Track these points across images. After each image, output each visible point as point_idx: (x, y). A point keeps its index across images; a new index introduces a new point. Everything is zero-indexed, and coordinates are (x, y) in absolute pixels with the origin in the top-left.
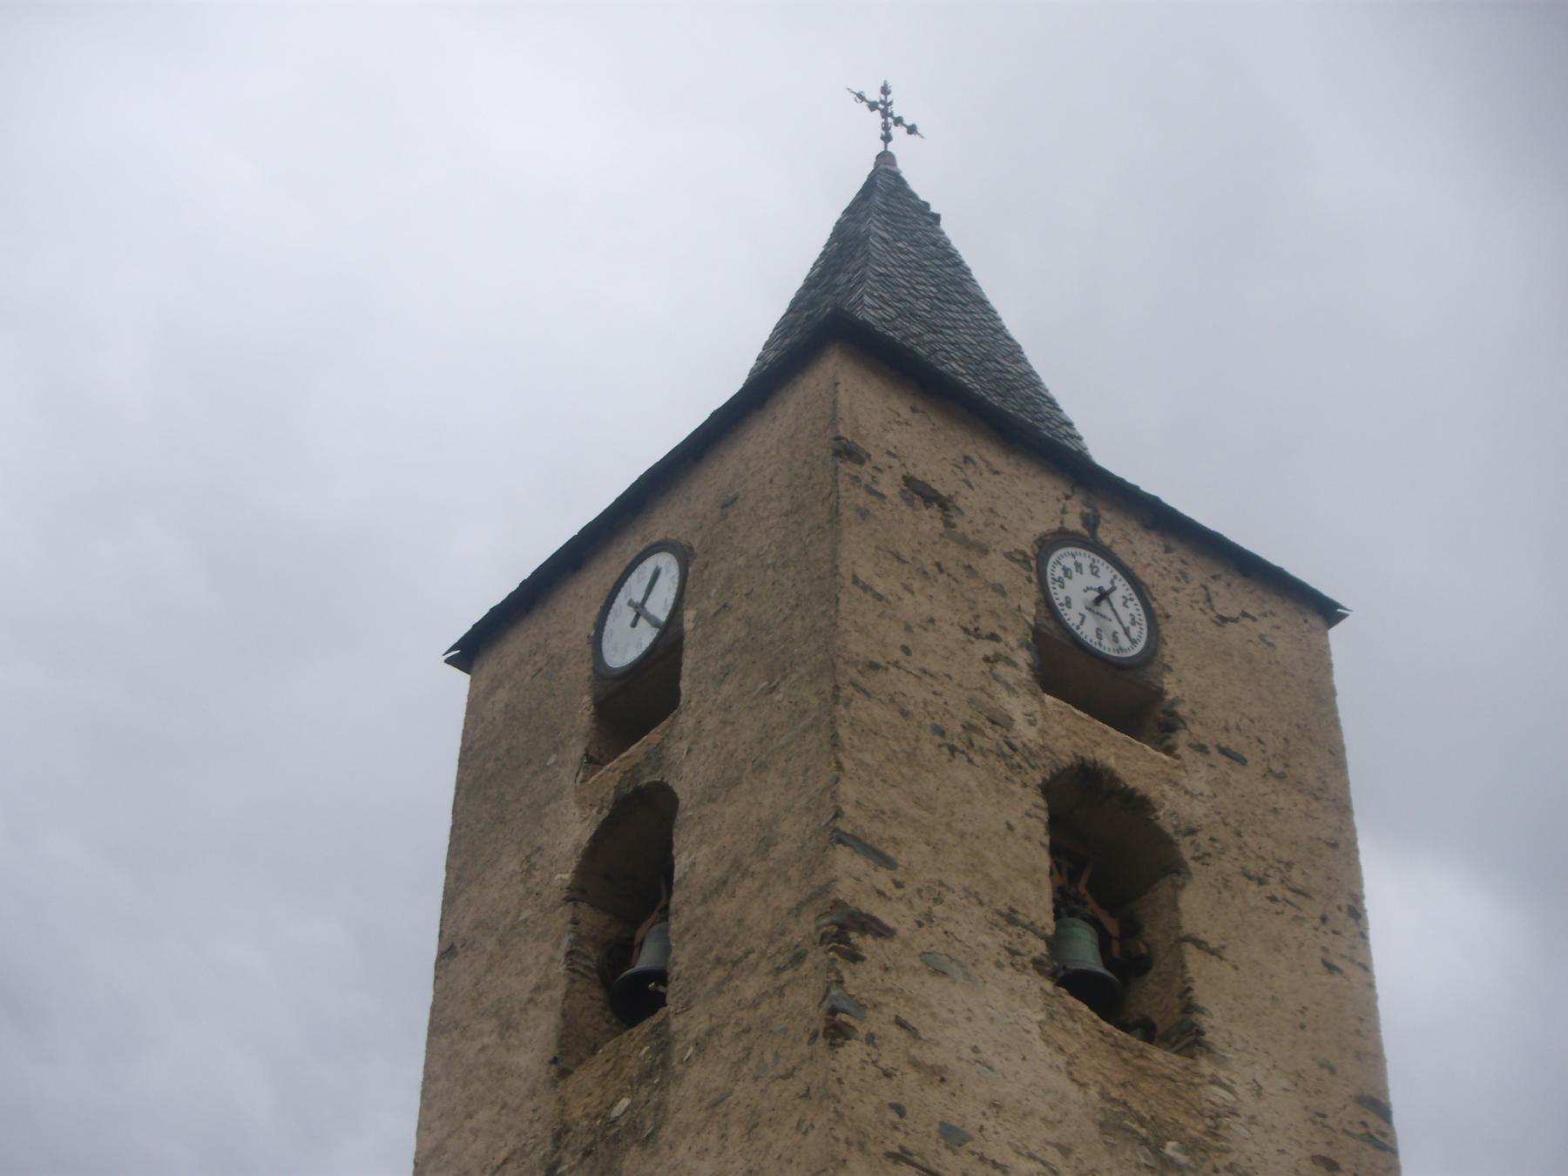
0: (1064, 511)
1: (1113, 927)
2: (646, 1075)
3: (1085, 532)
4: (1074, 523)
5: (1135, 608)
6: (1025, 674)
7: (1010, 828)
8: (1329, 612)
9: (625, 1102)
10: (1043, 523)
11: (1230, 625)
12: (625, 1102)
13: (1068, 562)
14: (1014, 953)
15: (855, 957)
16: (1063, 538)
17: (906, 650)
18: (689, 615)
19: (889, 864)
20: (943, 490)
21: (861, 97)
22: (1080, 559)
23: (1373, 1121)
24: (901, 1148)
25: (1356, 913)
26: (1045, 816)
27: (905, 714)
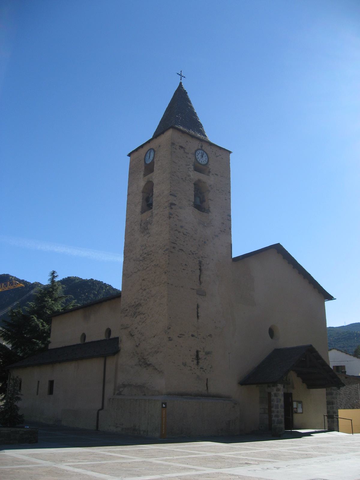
0: (198, 146)
2: (151, 216)
3: (201, 148)
4: (200, 147)
5: (206, 157)
6: (192, 169)
7: (190, 189)
8: (230, 152)
9: (148, 219)
11: (218, 157)
12: (148, 219)
14: (189, 205)
15: (172, 208)
16: (198, 149)
17: (179, 169)
18: (155, 160)
19: (176, 196)
20: (184, 146)
21: (178, 74)
22: (200, 152)
24: (176, 230)
25: (230, 192)
26: (194, 187)
27: (178, 177)
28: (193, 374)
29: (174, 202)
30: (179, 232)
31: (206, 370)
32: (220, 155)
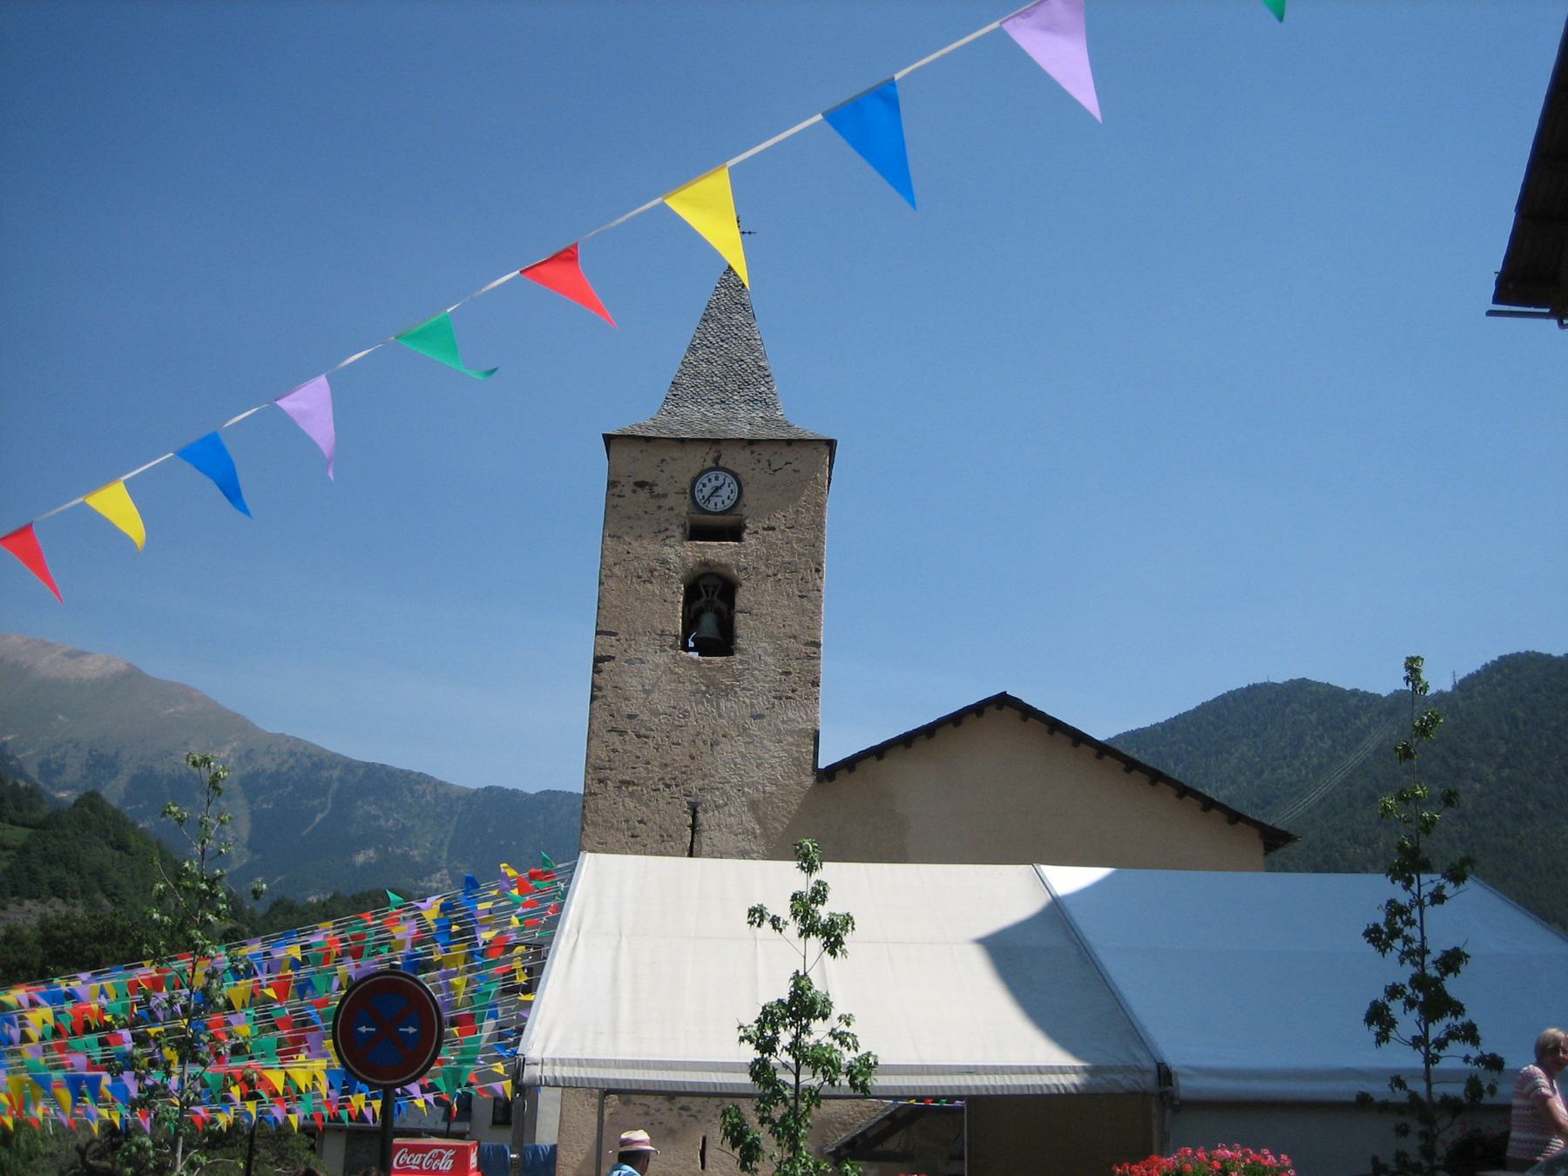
1: (724, 607)
3: (714, 465)
4: (709, 464)
5: (735, 486)
8: (831, 444)
10: (695, 471)
13: (706, 481)
23: (810, 650)
28: (652, 1124)
29: (612, 652)
30: (622, 733)
31: (699, 1111)
32: (787, 463)
